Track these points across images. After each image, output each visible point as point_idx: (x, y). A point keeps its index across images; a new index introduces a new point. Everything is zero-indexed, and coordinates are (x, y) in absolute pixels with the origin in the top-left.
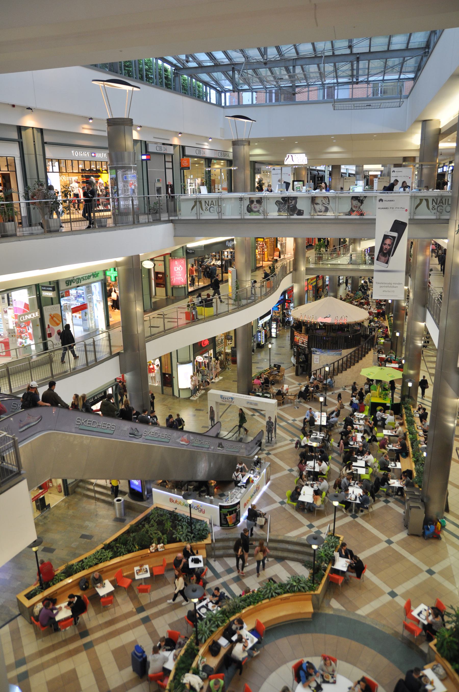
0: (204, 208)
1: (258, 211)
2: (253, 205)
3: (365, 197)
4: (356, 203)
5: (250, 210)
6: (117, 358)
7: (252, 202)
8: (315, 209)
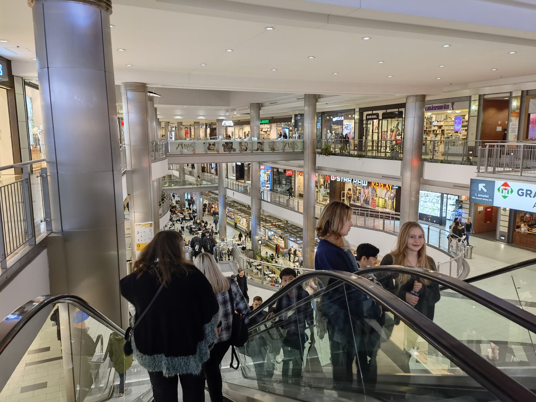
1: (214, 150)
2: (211, 147)
4: (259, 145)
5: (209, 149)
7: (210, 145)
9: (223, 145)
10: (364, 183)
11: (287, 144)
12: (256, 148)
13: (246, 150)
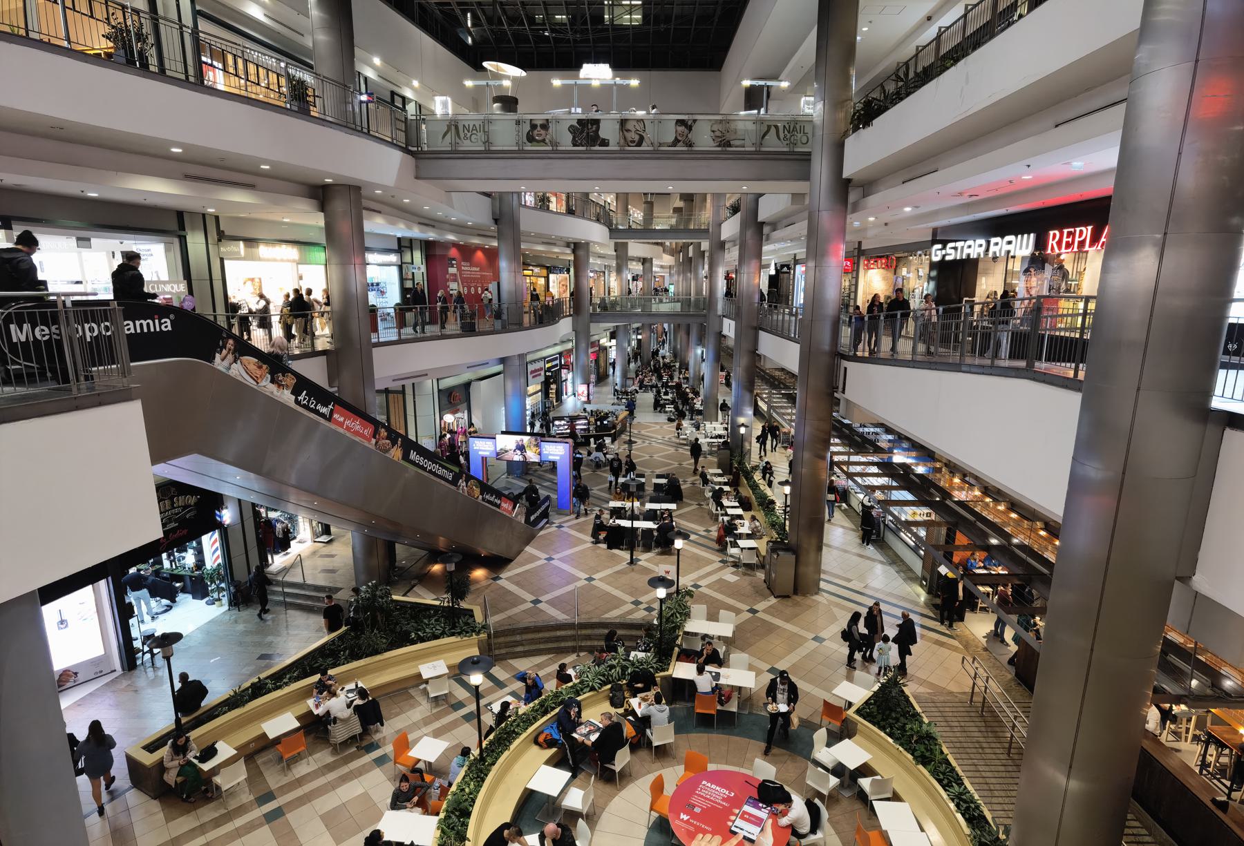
0: (462, 135)
1: (544, 141)
2: (536, 132)
3: (695, 121)
4: (681, 129)
5: (530, 139)
6: (323, 359)
7: (534, 127)
8: (625, 138)
9: (572, 129)
10: (1021, 248)
11: (773, 130)
12: (671, 139)
13: (639, 144)
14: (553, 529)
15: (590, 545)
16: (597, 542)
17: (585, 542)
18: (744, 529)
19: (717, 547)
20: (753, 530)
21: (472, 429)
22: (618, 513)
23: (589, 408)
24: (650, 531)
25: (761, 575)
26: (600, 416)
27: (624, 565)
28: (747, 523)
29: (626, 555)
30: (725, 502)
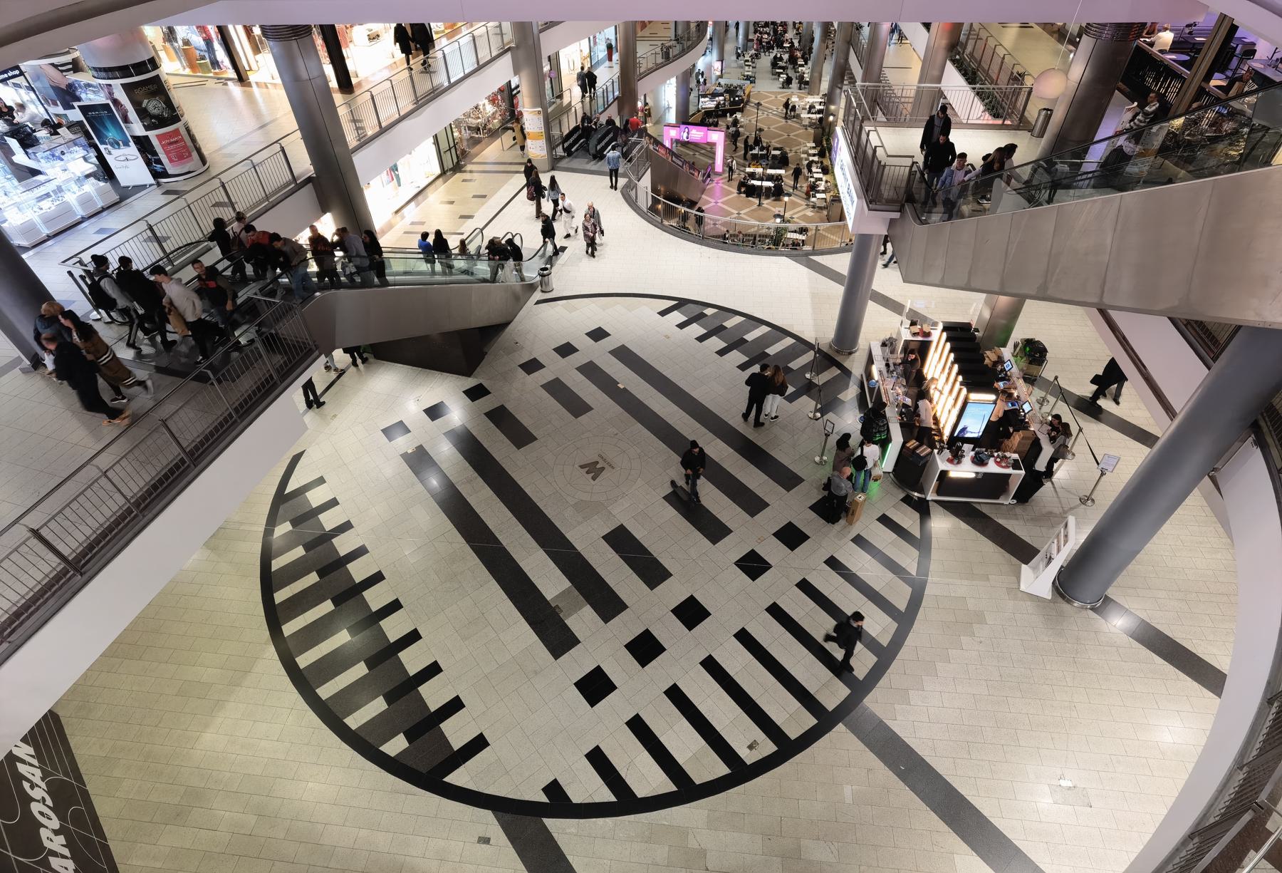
14: (714, 185)
15: (736, 195)
16: (740, 193)
17: (733, 193)
18: (822, 188)
19: (805, 197)
20: (826, 188)
21: (647, 107)
22: (752, 176)
23: (722, 82)
24: (770, 188)
25: (825, 212)
26: (731, 91)
27: (755, 206)
28: (823, 183)
29: (756, 201)
30: (814, 169)
